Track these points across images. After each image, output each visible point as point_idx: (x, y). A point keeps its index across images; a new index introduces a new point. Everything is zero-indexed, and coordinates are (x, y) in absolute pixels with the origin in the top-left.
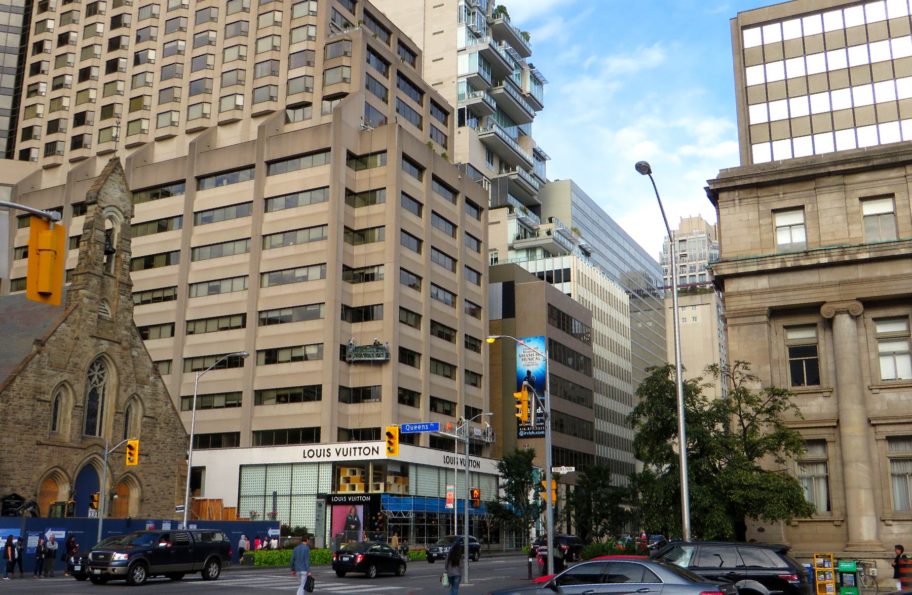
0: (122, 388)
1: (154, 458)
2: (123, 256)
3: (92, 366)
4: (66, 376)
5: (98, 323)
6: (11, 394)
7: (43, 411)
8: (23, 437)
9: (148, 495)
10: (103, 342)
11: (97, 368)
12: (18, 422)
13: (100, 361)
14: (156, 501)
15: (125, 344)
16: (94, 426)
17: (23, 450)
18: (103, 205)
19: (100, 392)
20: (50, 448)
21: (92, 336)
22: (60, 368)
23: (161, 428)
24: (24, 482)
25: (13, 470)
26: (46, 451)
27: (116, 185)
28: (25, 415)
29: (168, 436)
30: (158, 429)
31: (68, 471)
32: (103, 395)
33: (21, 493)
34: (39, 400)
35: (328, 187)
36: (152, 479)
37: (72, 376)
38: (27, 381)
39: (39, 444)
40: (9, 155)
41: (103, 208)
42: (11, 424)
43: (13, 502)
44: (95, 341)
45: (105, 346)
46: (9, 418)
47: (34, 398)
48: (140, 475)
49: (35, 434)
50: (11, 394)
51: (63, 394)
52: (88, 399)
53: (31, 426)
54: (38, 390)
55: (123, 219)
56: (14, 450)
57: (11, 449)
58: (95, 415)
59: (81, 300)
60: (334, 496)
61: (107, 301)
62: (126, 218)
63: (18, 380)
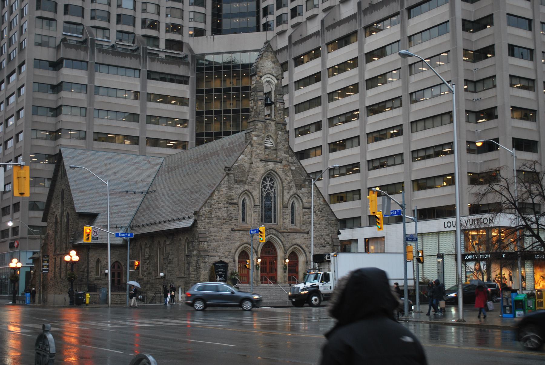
0: (285, 192)
2: (278, 106)
3: (265, 179)
4: (247, 187)
5: (265, 151)
6: (213, 202)
7: (235, 211)
8: (223, 227)
10: (269, 163)
11: (268, 180)
12: (219, 218)
13: (269, 176)
15: (284, 163)
16: (270, 217)
17: (224, 234)
18: (261, 74)
19: (272, 194)
20: (241, 232)
21: (261, 161)
22: (242, 182)
24: (228, 253)
25: (219, 246)
26: (237, 235)
27: (269, 60)
28: (223, 213)
29: (322, 220)
32: (275, 197)
33: (225, 260)
34: (230, 204)
35: (448, 21)
37: (250, 187)
38: (222, 193)
39: (233, 230)
40: (258, 30)
41: (261, 77)
42: (215, 220)
43: (221, 265)
44: (264, 163)
45: (271, 165)
46: (213, 216)
47: (227, 202)
48: (304, 246)
49: (230, 225)
50: (213, 202)
51: (247, 199)
52: (264, 200)
53: (229, 219)
54: (230, 197)
55: (276, 81)
56: (218, 235)
57: (216, 234)
58: (270, 210)
59: (252, 139)
60: (466, 255)
61: (271, 136)
62: (278, 80)
63: (216, 193)
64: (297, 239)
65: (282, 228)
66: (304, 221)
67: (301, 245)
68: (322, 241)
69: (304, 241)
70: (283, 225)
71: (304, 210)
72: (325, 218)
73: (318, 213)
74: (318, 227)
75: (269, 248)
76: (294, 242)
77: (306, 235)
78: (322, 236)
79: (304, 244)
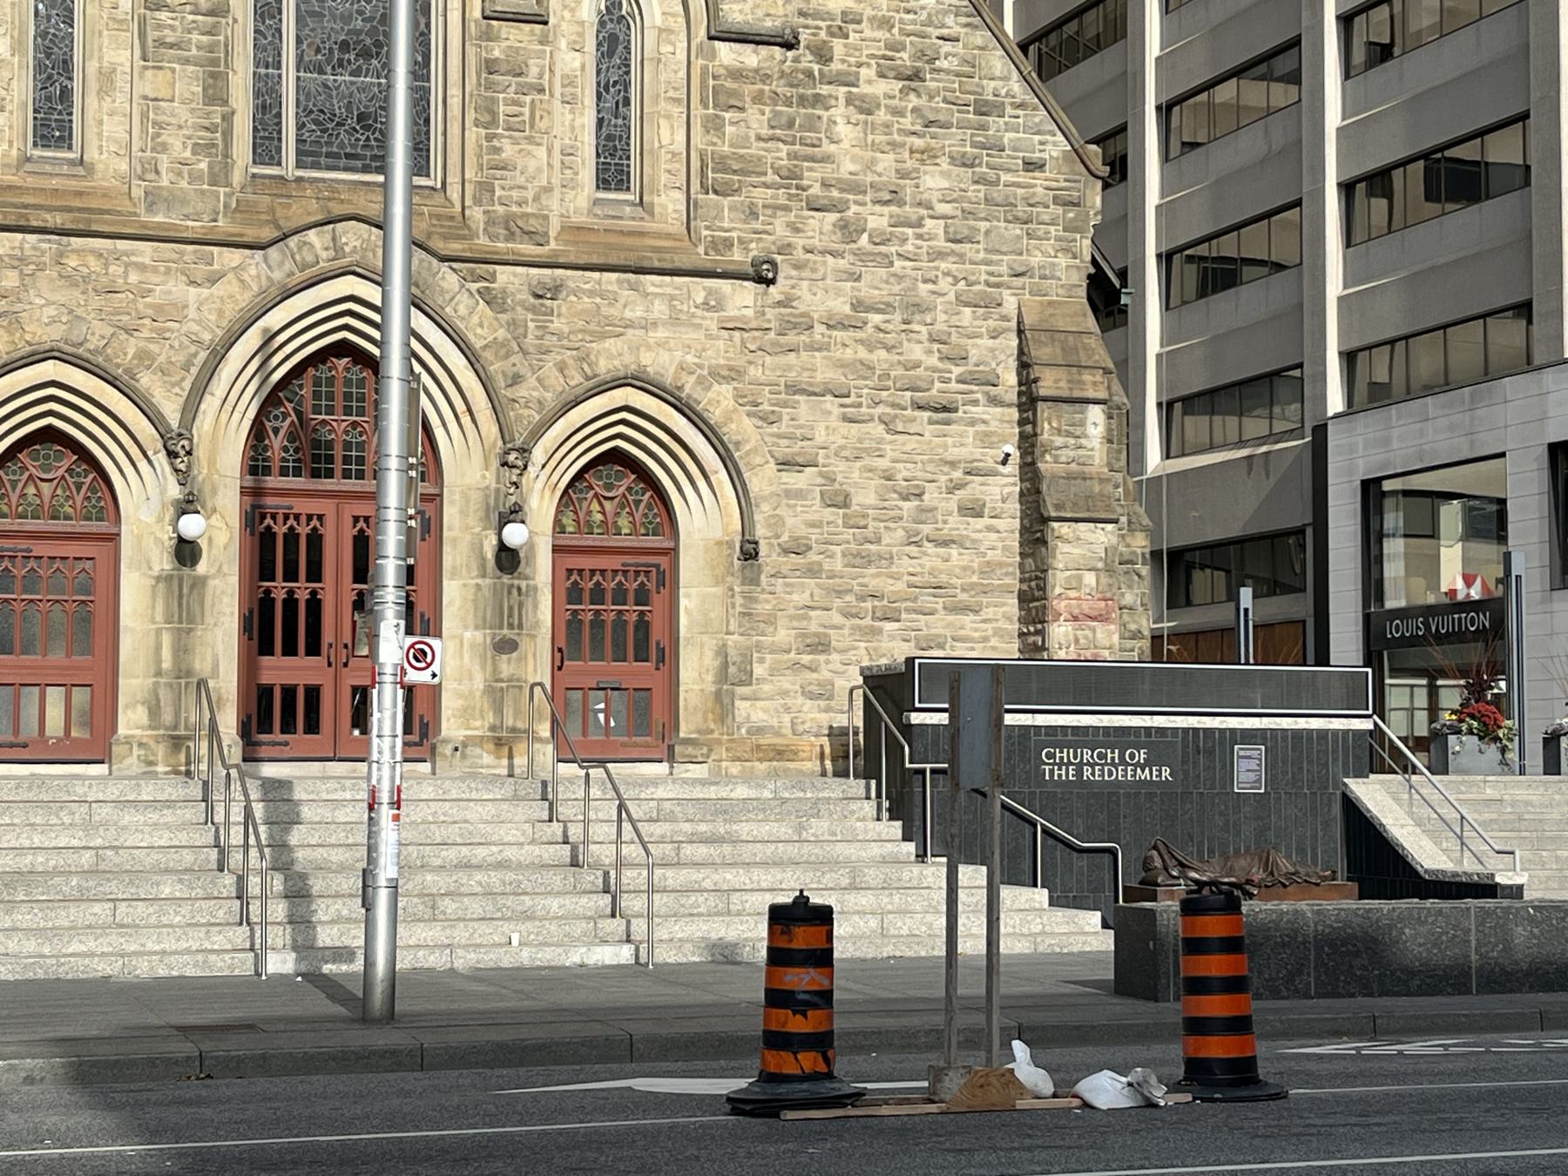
1: (822, 297)
9: (790, 510)
14: (861, 560)
16: (373, 122)
23: (865, 107)
30: (839, 112)
31: (146, 381)
36: (823, 425)
48: (719, 401)
58: (376, 48)
64: (647, 325)
65: (476, 215)
66: (722, 164)
67: (689, 387)
68: (916, 352)
69: (721, 351)
70: (486, 188)
71: (727, 53)
72: (955, 141)
73: (882, 88)
74: (878, 219)
75: (317, 412)
76: (610, 357)
77: (742, 298)
78: (918, 307)
79: (717, 375)
